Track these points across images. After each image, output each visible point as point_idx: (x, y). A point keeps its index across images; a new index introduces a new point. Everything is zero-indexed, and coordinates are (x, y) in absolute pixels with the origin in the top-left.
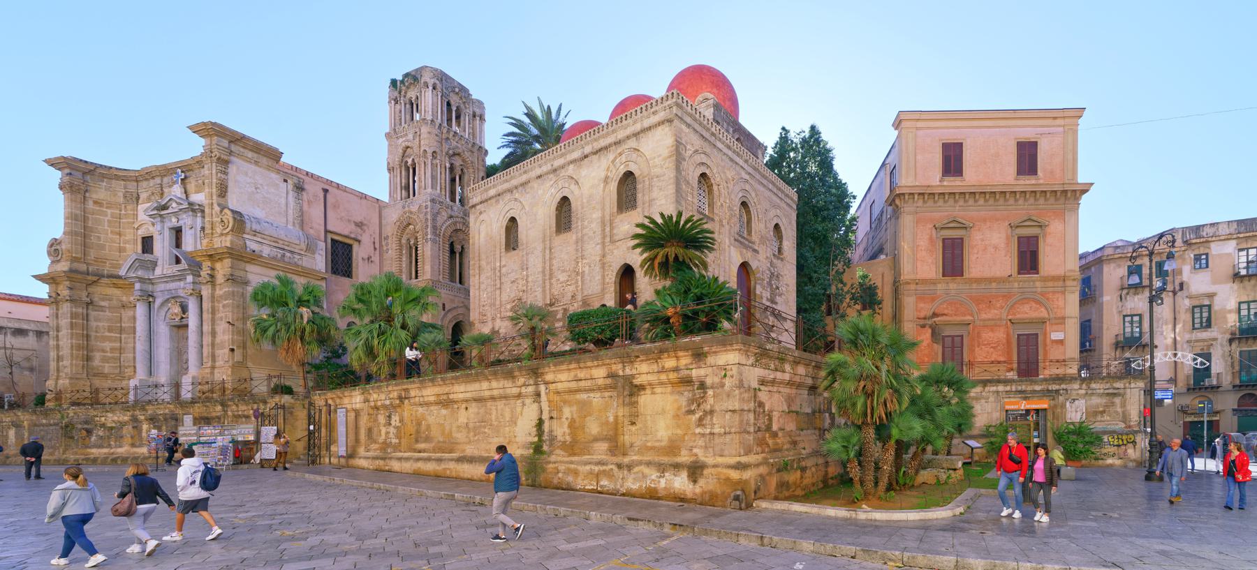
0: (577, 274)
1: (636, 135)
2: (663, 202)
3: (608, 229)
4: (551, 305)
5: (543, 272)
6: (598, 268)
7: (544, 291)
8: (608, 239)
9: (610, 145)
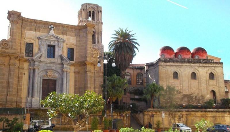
0: (199, 89)
1: (214, 67)
2: (221, 81)
3: (207, 82)
4: (191, 94)
5: (188, 87)
6: (206, 90)
7: (189, 91)
8: (208, 84)
9: (207, 66)
